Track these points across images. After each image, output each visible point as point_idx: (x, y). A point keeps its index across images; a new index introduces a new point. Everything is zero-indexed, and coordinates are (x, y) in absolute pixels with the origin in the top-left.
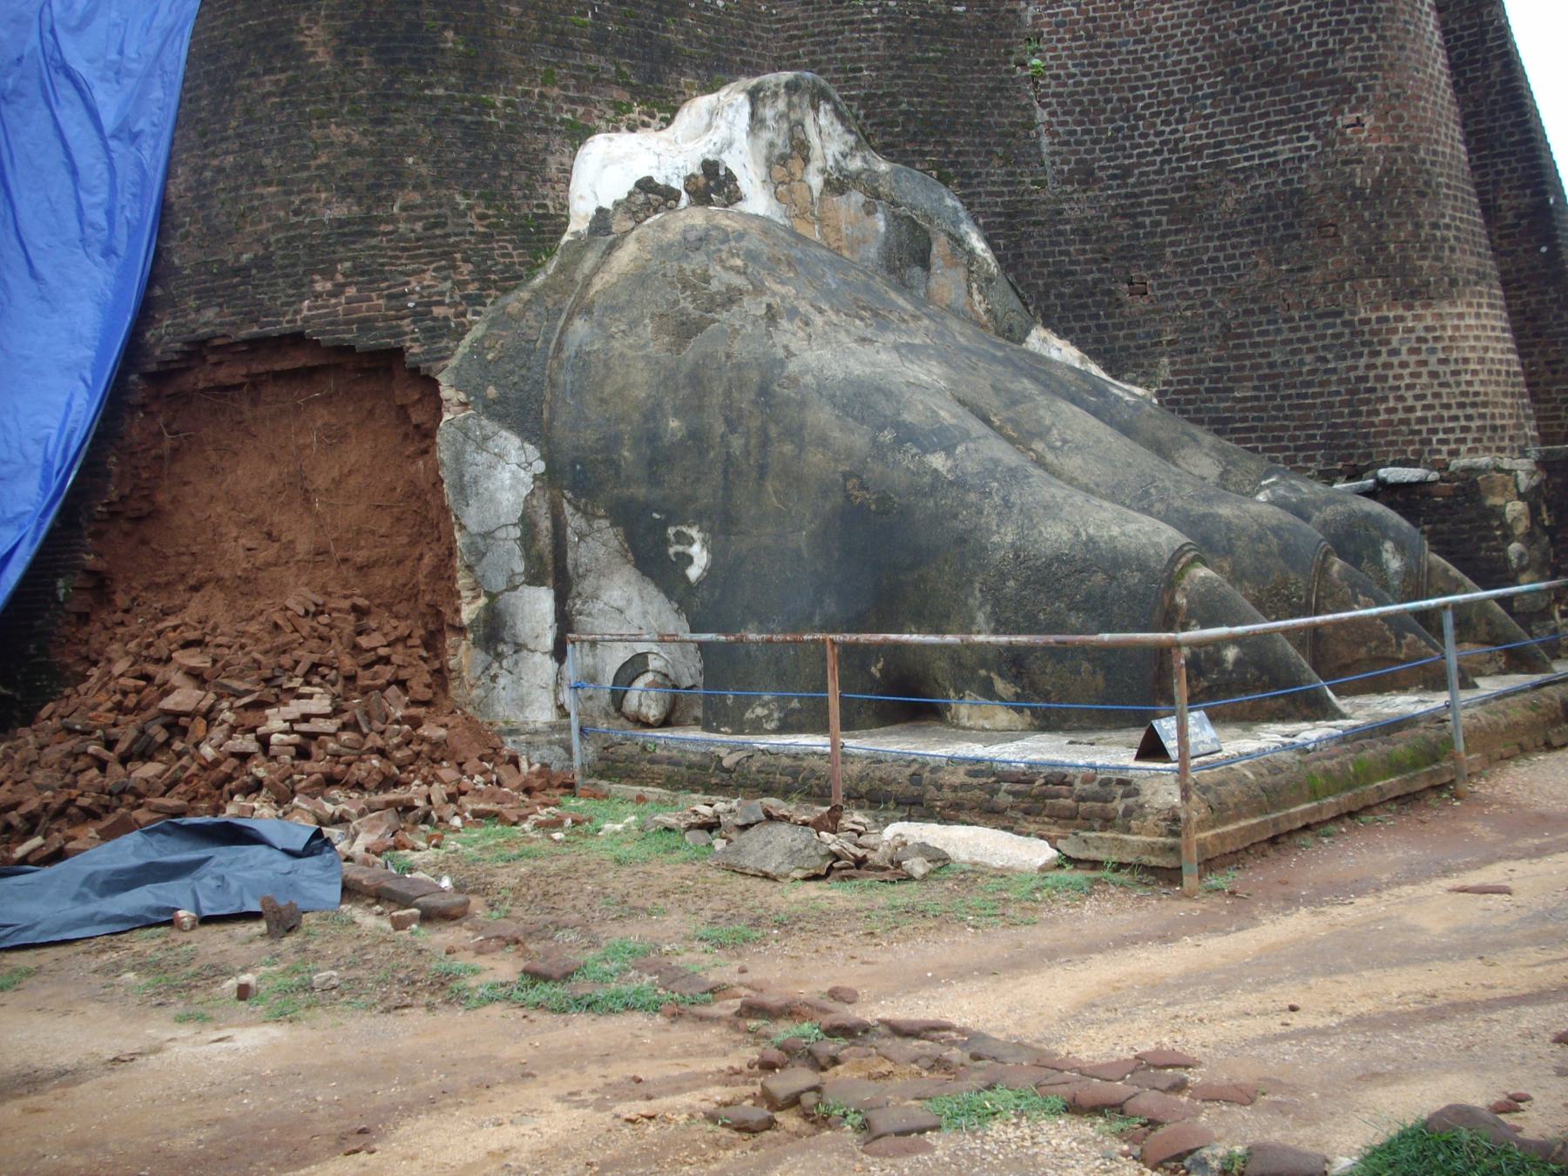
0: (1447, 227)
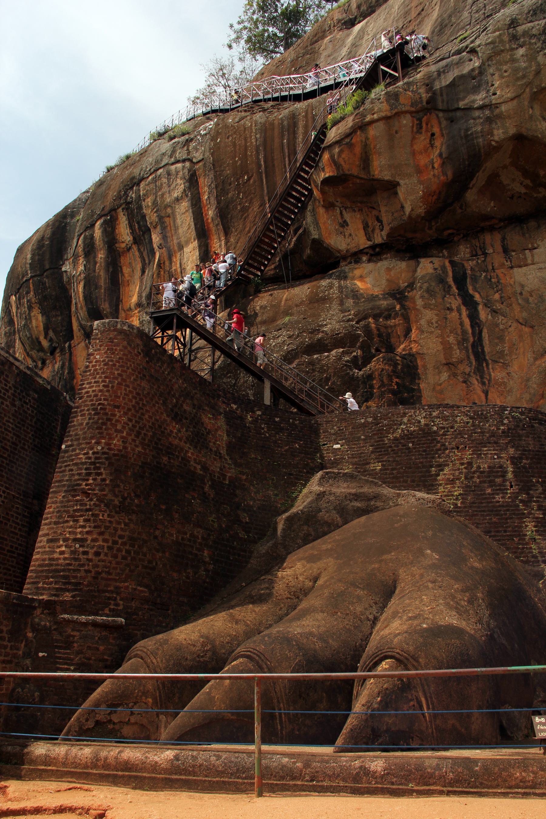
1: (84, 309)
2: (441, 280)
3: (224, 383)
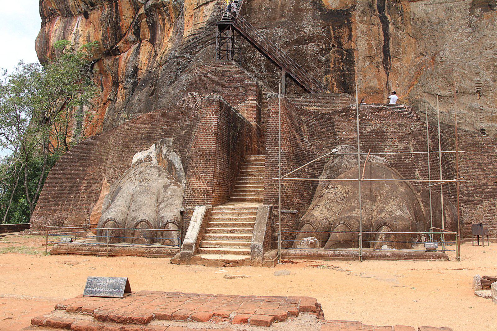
0: (198, 163)
2: (371, 6)
3: (247, 56)
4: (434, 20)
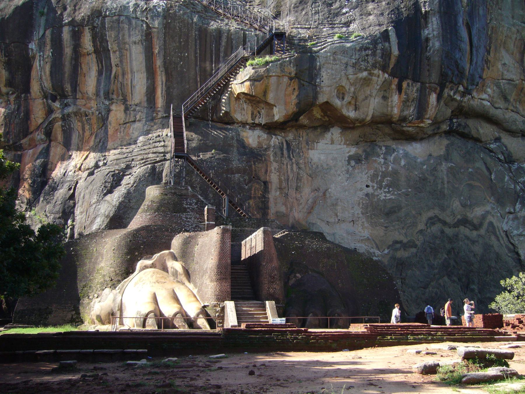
1: (49, 82)
2: (282, 149)
4: (325, 166)
